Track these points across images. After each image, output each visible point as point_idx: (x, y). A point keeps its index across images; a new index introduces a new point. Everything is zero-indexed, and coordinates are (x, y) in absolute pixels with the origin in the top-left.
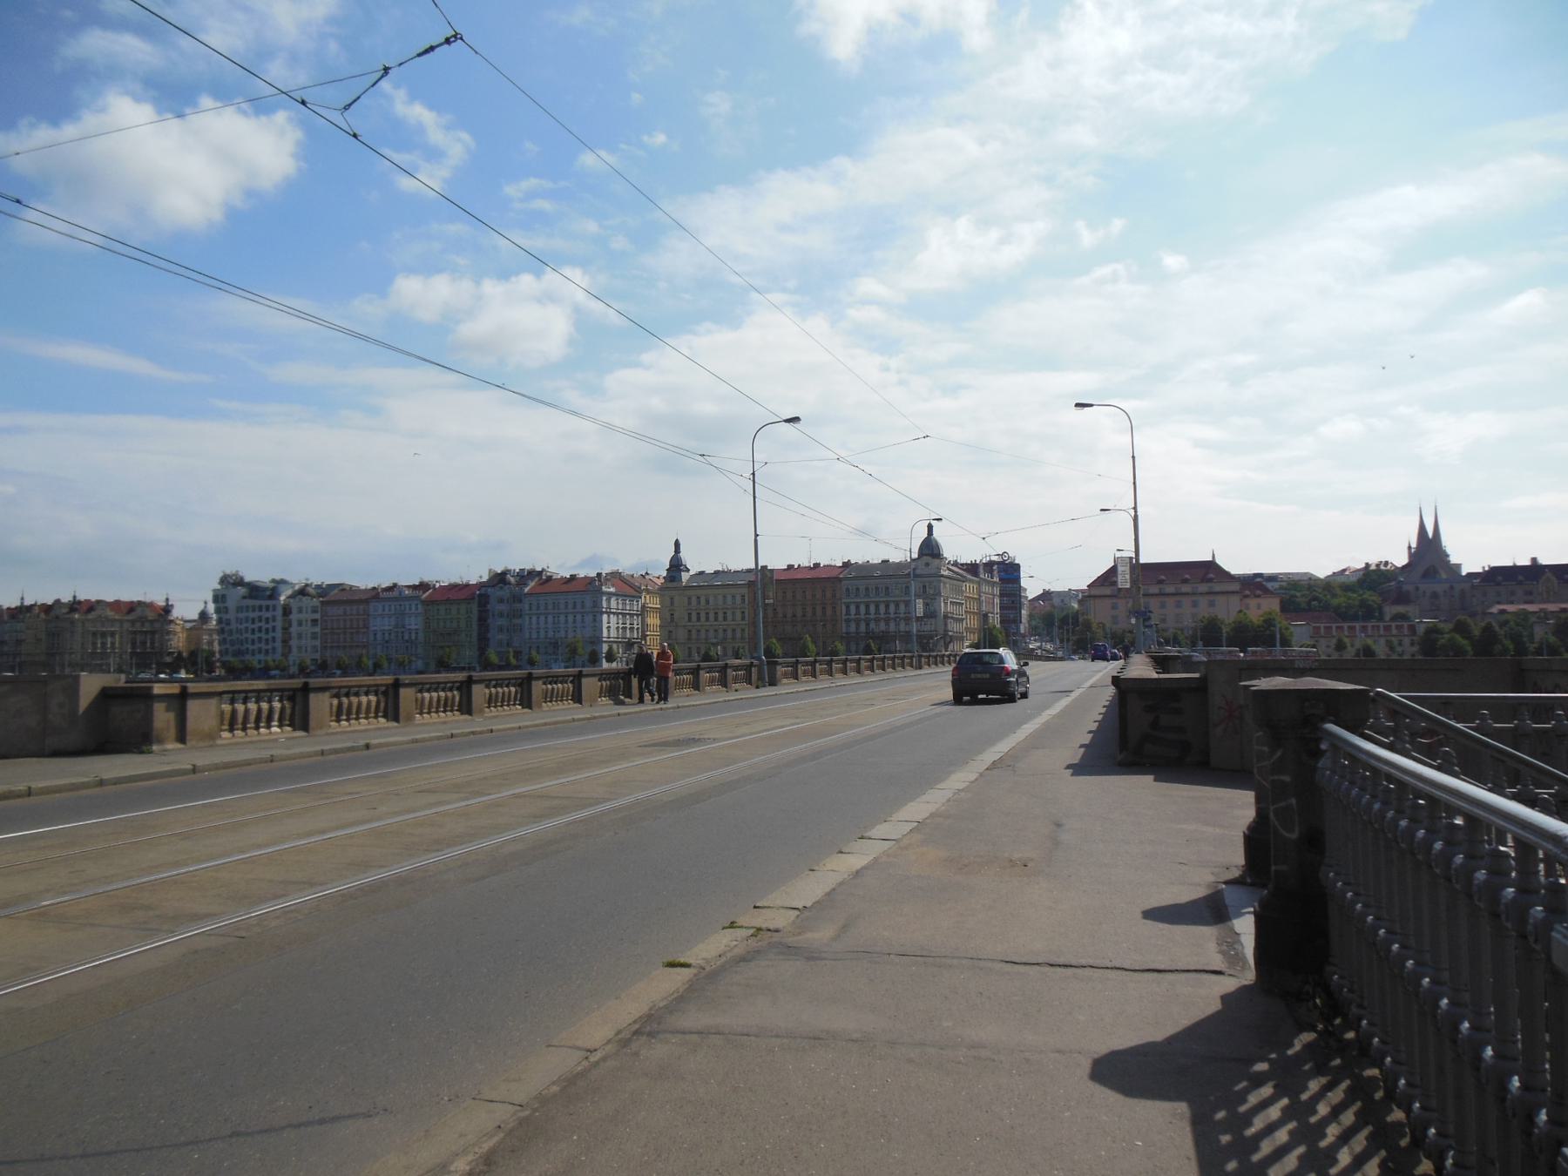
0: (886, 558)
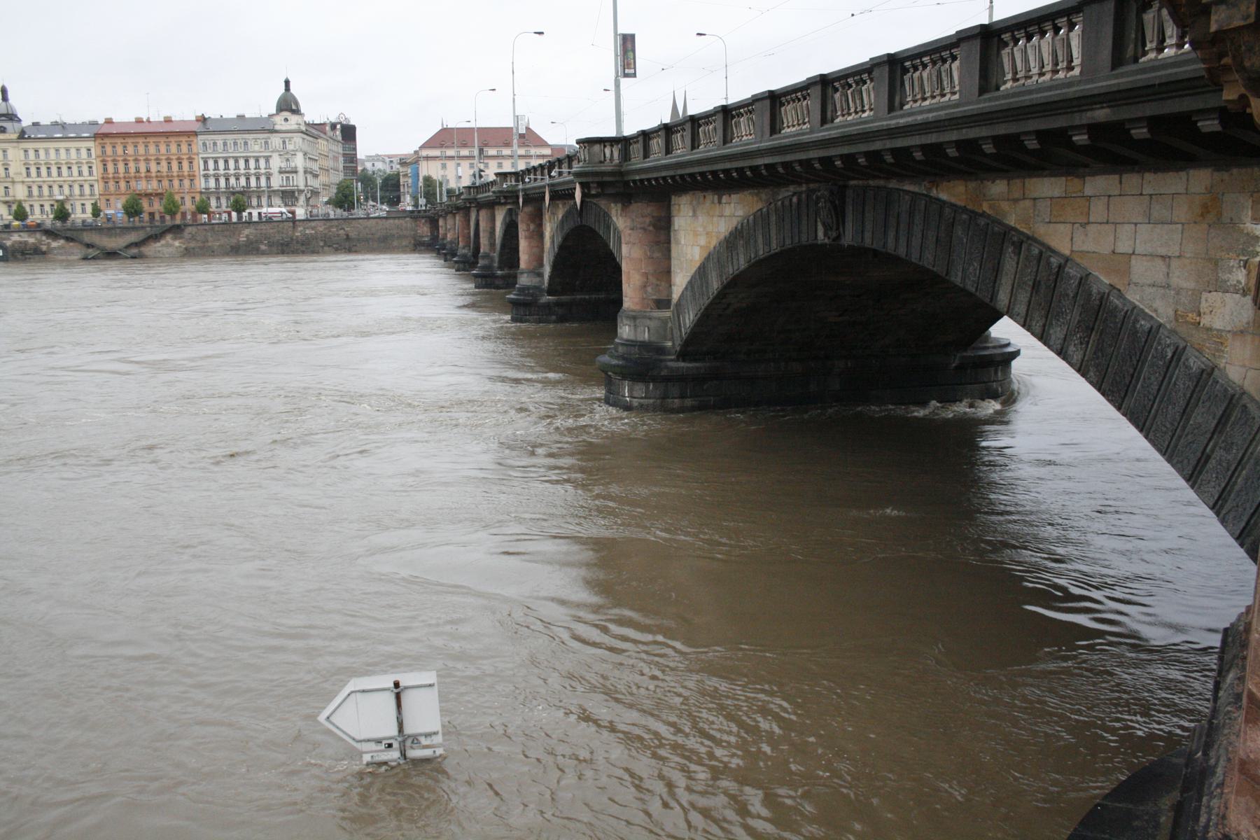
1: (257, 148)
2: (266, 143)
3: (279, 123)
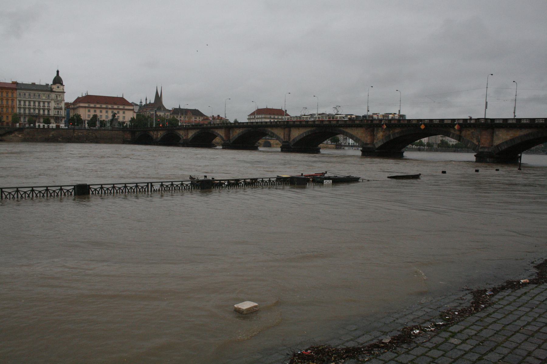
0: (33, 82)
1: (44, 98)
2: (49, 96)
3: (55, 88)
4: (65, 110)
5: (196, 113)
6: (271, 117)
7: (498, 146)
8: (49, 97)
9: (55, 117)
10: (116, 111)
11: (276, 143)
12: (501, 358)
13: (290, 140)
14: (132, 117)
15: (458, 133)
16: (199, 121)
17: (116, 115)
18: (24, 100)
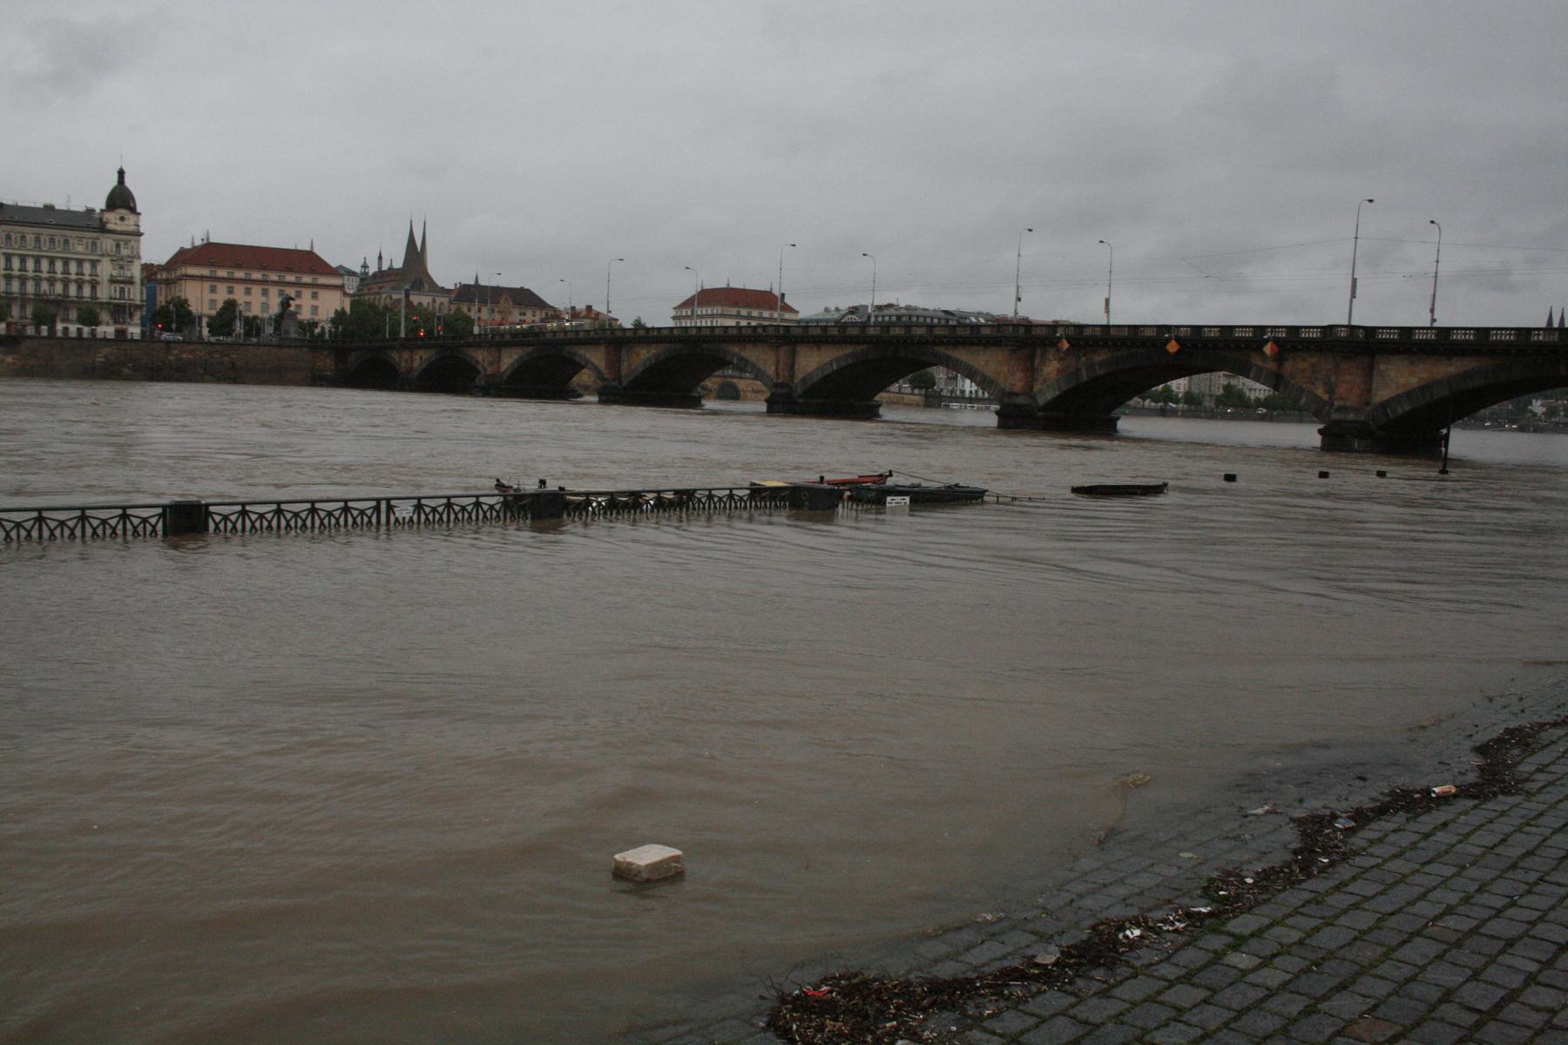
0: (48, 201)
1: (80, 248)
3: (112, 219)
4: (142, 284)
5: (524, 298)
6: (739, 312)
7: (1384, 405)
8: (96, 246)
9: (111, 307)
10: (291, 292)
11: (755, 388)
12: (1369, 1009)
13: (793, 382)
14: (339, 309)
15: (1271, 366)
16: (533, 322)
17: (291, 302)
18: (22, 255)
